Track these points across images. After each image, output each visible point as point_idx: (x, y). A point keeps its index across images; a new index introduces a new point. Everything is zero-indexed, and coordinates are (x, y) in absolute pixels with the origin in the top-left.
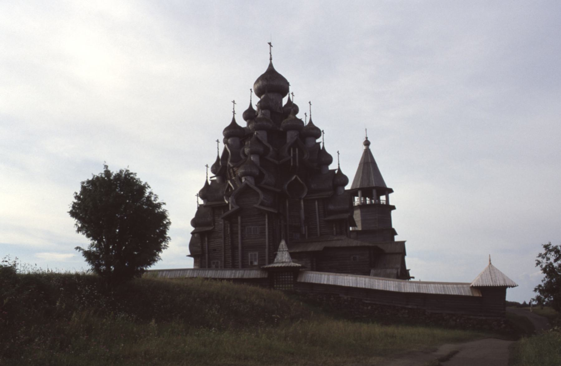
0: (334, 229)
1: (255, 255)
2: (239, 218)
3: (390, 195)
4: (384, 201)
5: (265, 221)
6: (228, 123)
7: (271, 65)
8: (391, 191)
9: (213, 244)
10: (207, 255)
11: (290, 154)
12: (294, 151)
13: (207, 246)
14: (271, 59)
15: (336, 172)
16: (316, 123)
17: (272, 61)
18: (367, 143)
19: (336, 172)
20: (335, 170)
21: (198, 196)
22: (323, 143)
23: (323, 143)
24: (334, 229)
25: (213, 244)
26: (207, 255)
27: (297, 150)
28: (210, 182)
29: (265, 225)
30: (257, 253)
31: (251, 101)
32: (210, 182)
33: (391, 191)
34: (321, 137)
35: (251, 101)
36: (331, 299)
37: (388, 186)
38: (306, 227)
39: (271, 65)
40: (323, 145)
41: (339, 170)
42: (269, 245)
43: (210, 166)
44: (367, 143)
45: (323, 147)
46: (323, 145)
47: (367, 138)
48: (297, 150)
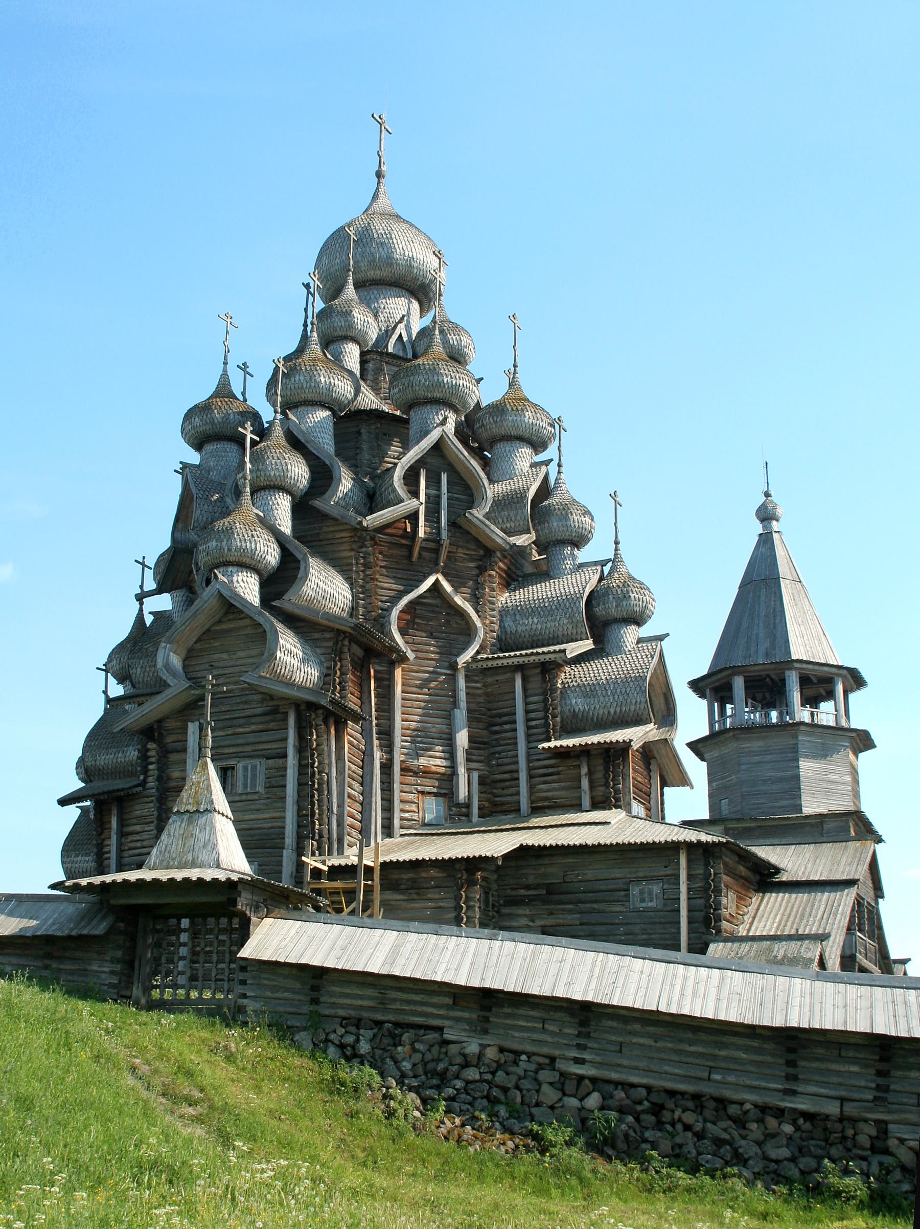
0: (585, 783)
5: (285, 739)
6: (203, 392)
8: (855, 680)
9: (139, 844)
11: (415, 494)
12: (434, 482)
13: (114, 849)
21: (106, 671)
22: (559, 465)
23: (559, 465)
24: (585, 783)
25: (139, 844)
27: (444, 477)
28: (149, 620)
32: (149, 620)
33: (855, 680)
36: (400, 1048)
38: (475, 775)
43: (151, 562)
47: (767, 495)
48: (444, 477)
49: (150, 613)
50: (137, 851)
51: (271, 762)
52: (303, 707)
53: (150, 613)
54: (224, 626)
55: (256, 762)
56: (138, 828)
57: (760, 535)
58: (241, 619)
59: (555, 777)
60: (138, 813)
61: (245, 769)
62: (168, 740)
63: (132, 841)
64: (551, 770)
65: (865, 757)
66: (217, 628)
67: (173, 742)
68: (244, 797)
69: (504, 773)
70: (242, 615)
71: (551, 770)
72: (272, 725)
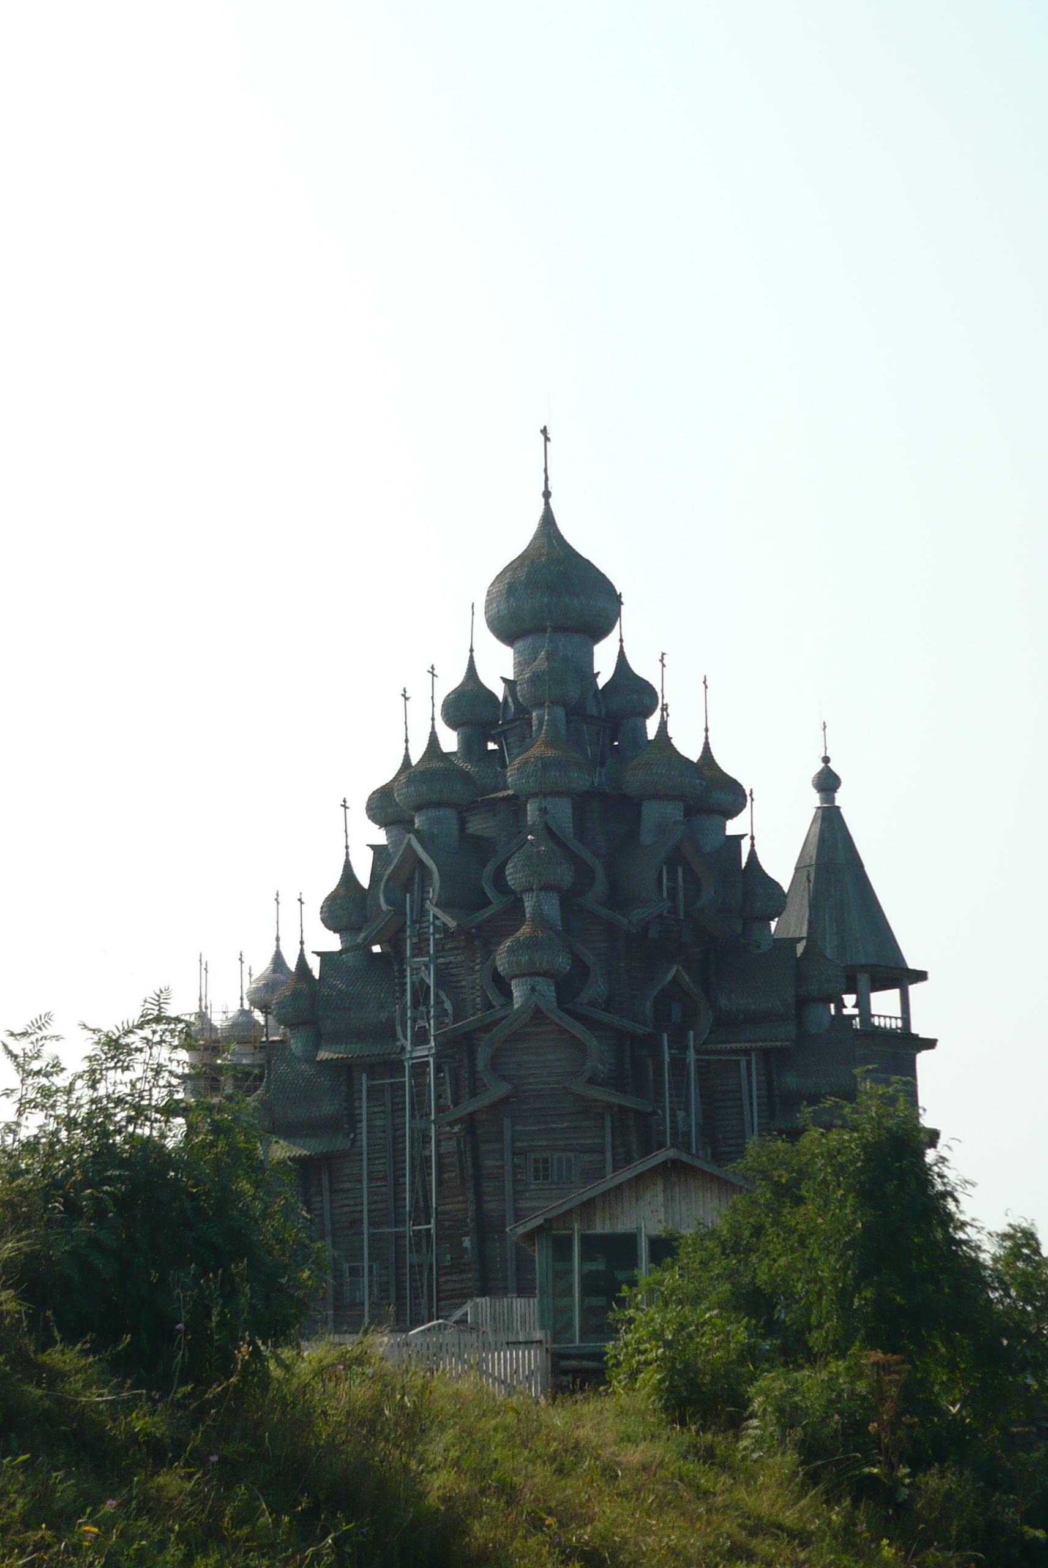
2: (507, 1122)
3: (914, 989)
4: (896, 1018)
9: (352, 1202)
14: (547, 495)
16: (728, 763)
18: (827, 782)
19: (800, 948)
20: (799, 940)
22: (752, 838)
23: (752, 838)
27: (680, 871)
28: (314, 964)
31: (471, 650)
34: (745, 814)
35: (471, 650)
37: (913, 963)
40: (753, 845)
44: (827, 782)
45: (753, 854)
46: (753, 845)
47: (826, 760)
48: (680, 871)
51: (586, 1157)
52: (615, 1109)
54: (529, 1030)
55: (571, 1155)
56: (348, 1185)
57: (818, 808)
58: (548, 1024)
60: (348, 1171)
61: (560, 1160)
65: (923, 1059)
70: (548, 1021)
72: (586, 1123)
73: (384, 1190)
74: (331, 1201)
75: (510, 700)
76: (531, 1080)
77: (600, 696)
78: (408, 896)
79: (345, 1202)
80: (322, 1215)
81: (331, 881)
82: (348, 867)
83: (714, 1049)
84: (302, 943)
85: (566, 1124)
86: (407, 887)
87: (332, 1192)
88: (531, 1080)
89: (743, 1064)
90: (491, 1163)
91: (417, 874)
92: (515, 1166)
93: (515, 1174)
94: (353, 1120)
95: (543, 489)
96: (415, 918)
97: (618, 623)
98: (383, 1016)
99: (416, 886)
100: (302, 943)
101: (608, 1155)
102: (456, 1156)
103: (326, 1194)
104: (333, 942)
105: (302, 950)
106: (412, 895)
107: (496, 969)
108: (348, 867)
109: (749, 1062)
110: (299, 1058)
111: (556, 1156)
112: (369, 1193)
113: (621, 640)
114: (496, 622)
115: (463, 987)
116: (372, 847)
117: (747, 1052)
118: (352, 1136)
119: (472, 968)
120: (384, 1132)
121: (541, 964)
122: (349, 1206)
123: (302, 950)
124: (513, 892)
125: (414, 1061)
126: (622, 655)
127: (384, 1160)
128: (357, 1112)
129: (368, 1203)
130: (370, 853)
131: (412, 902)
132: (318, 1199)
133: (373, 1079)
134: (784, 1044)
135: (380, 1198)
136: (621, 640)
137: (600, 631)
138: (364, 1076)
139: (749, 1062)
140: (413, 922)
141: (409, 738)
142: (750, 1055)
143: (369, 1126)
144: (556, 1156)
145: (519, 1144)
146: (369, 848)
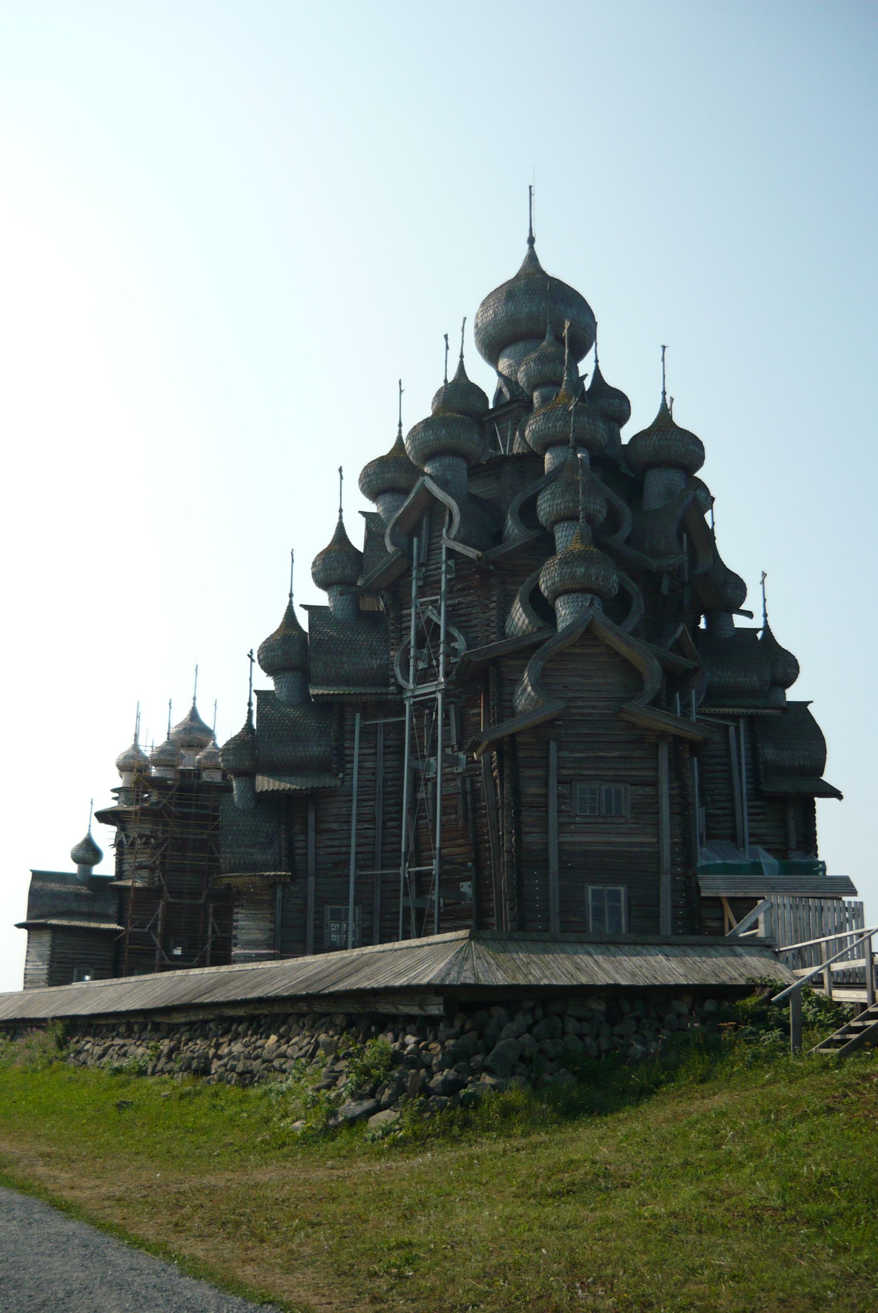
1: (615, 896)
2: (553, 746)
7: (532, 258)
9: (336, 843)
10: (311, 880)
14: (531, 241)
15: (759, 635)
17: (536, 246)
20: (757, 630)
25: (336, 843)
26: (311, 880)
27: (685, 536)
29: (655, 784)
30: (622, 889)
31: (462, 356)
35: (462, 356)
39: (532, 258)
41: (766, 629)
42: (674, 864)
48: (685, 536)
49: (301, 606)
50: (334, 850)
51: (639, 790)
53: (301, 606)
54: (579, 650)
56: (335, 826)
59: (762, 817)
61: (608, 792)
62: (521, 754)
63: (328, 839)
64: (758, 811)
66: (573, 651)
67: (524, 757)
68: (609, 820)
69: (719, 809)
71: (758, 811)
73: (371, 832)
74: (316, 840)
75: (505, 390)
76: (579, 704)
77: (586, 396)
78: (415, 540)
79: (330, 843)
80: (306, 855)
81: (325, 539)
82: (341, 528)
83: (707, 711)
84: (291, 595)
85: (616, 754)
86: (415, 531)
87: (318, 831)
88: (579, 704)
89: (732, 730)
90: (533, 790)
91: (425, 520)
92: (560, 796)
93: (559, 804)
94: (341, 758)
95: (527, 235)
96: (421, 561)
97: (594, 344)
98: (375, 663)
99: (424, 532)
100: (291, 595)
101: (664, 788)
102: (460, 797)
103: (311, 834)
104: (322, 598)
105: (291, 602)
106: (419, 541)
107: (537, 587)
108: (341, 528)
109: (737, 729)
110: (282, 703)
111: (604, 788)
112: (358, 836)
113: (597, 361)
114: (490, 328)
115: (475, 626)
116: (364, 514)
117: (735, 718)
118: (341, 775)
119: (487, 606)
120: (374, 774)
121: (597, 578)
122: (332, 846)
123: (291, 602)
124: (541, 527)
125: (415, 700)
126: (597, 373)
127: (372, 803)
128: (347, 752)
129: (357, 846)
130: (362, 521)
131: (419, 548)
132: (302, 838)
133: (366, 720)
134: (774, 712)
135: (366, 840)
136: (597, 361)
137: (579, 352)
138: (358, 716)
139: (737, 729)
140: (420, 565)
141: (402, 422)
142: (738, 722)
143: (360, 767)
144: (604, 788)
145: (564, 772)
146: (360, 516)
